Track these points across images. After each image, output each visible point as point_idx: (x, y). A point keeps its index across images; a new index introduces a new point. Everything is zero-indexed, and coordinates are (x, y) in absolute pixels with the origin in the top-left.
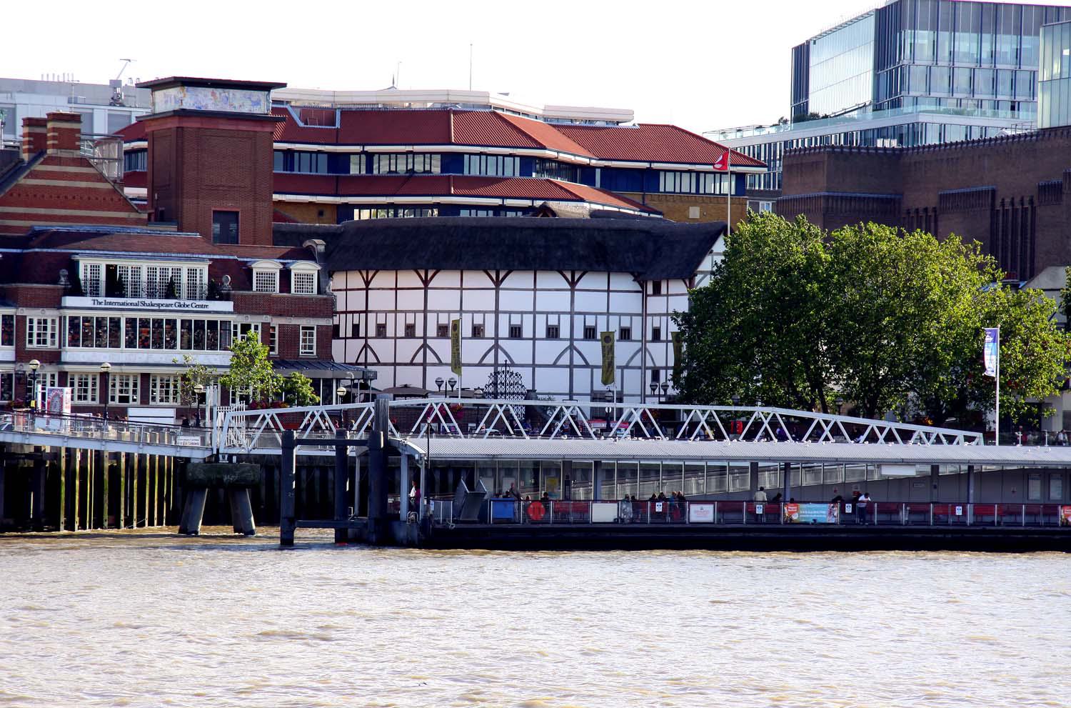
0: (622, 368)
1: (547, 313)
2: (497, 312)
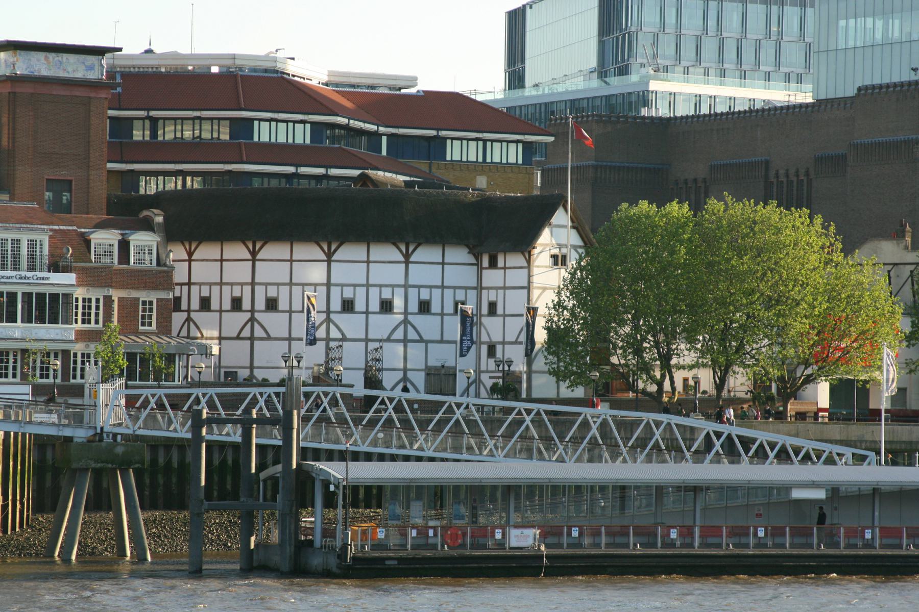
1: (381, 286)
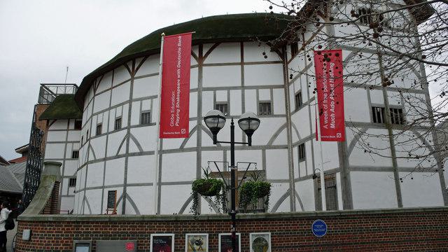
0: (264, 148)
2: (130, 101)
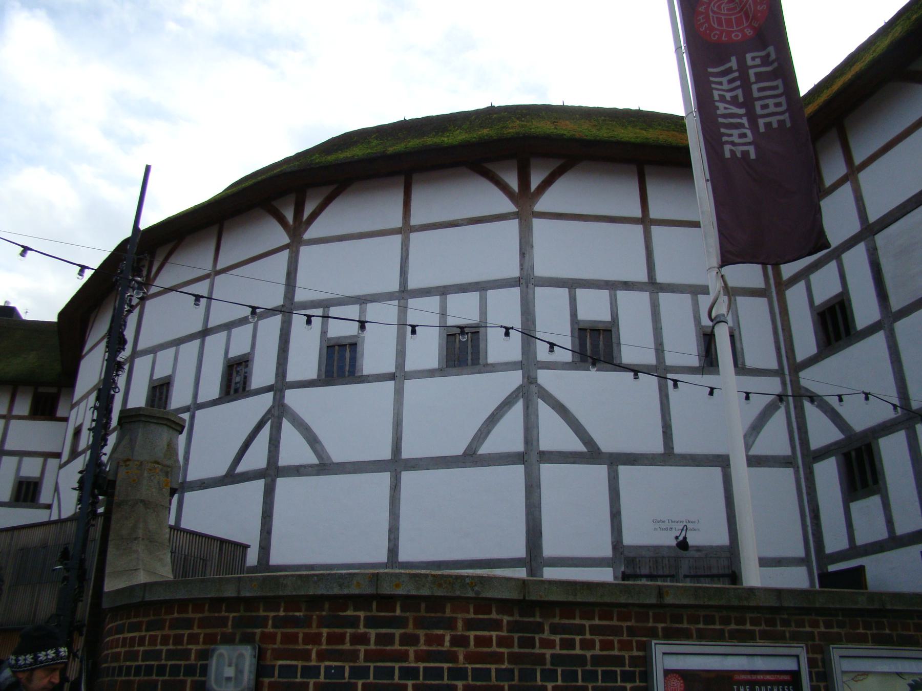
1: (444, 291)
